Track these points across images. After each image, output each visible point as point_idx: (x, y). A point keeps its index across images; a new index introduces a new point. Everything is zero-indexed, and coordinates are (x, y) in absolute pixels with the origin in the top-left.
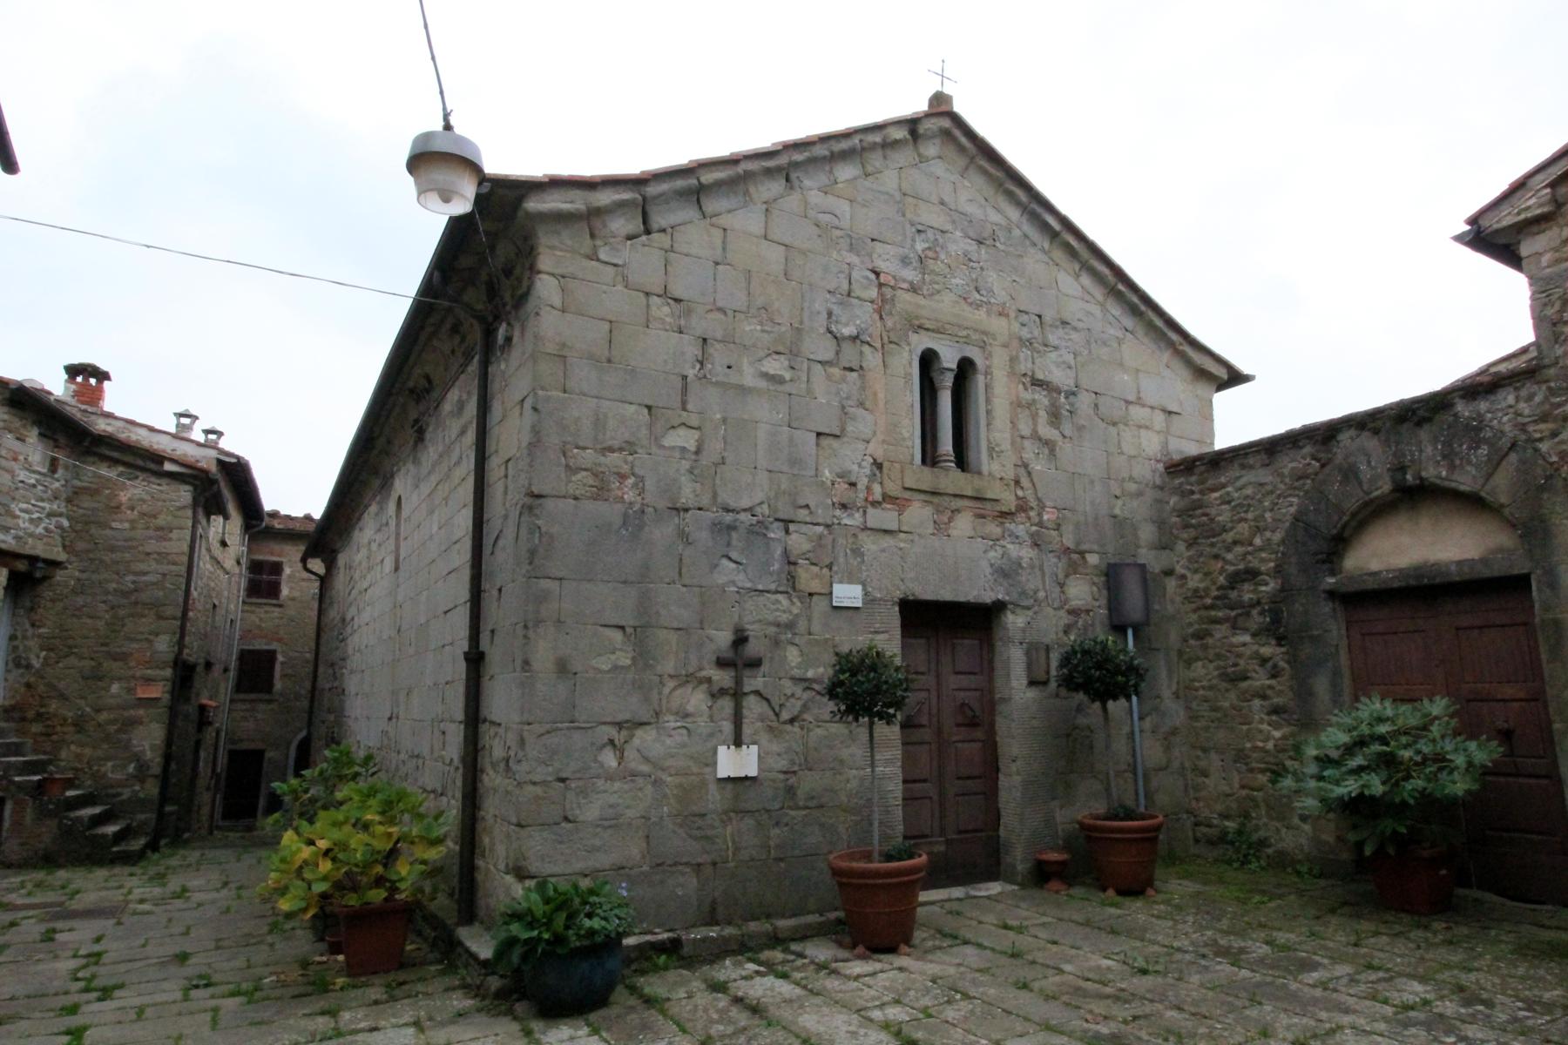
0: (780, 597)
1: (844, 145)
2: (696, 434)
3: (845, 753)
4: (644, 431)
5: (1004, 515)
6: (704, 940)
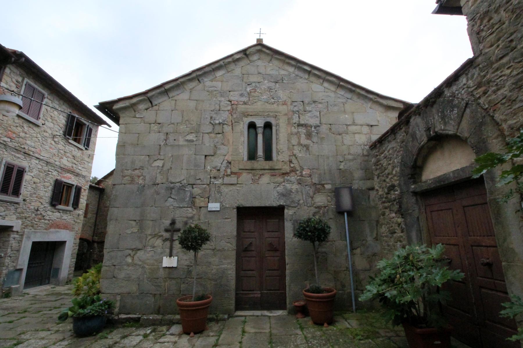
0: (189, 209)
1: (217, 65)
2: (163, 161)
3: (211, 260)
6: (147, 319)
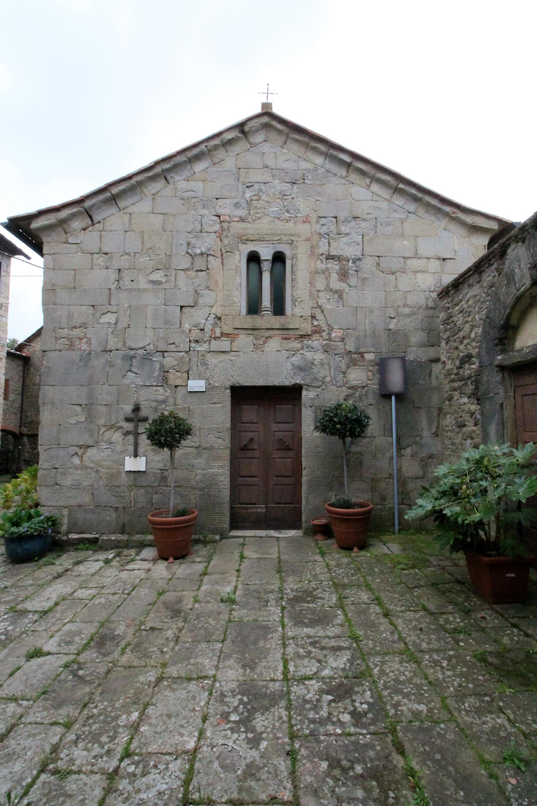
0: (159, 388)
1: (195, 151)
2: (115, 315)
3: (195, 462)
4: (91, 317)
5: (302, 336)
6: (108, 540)
